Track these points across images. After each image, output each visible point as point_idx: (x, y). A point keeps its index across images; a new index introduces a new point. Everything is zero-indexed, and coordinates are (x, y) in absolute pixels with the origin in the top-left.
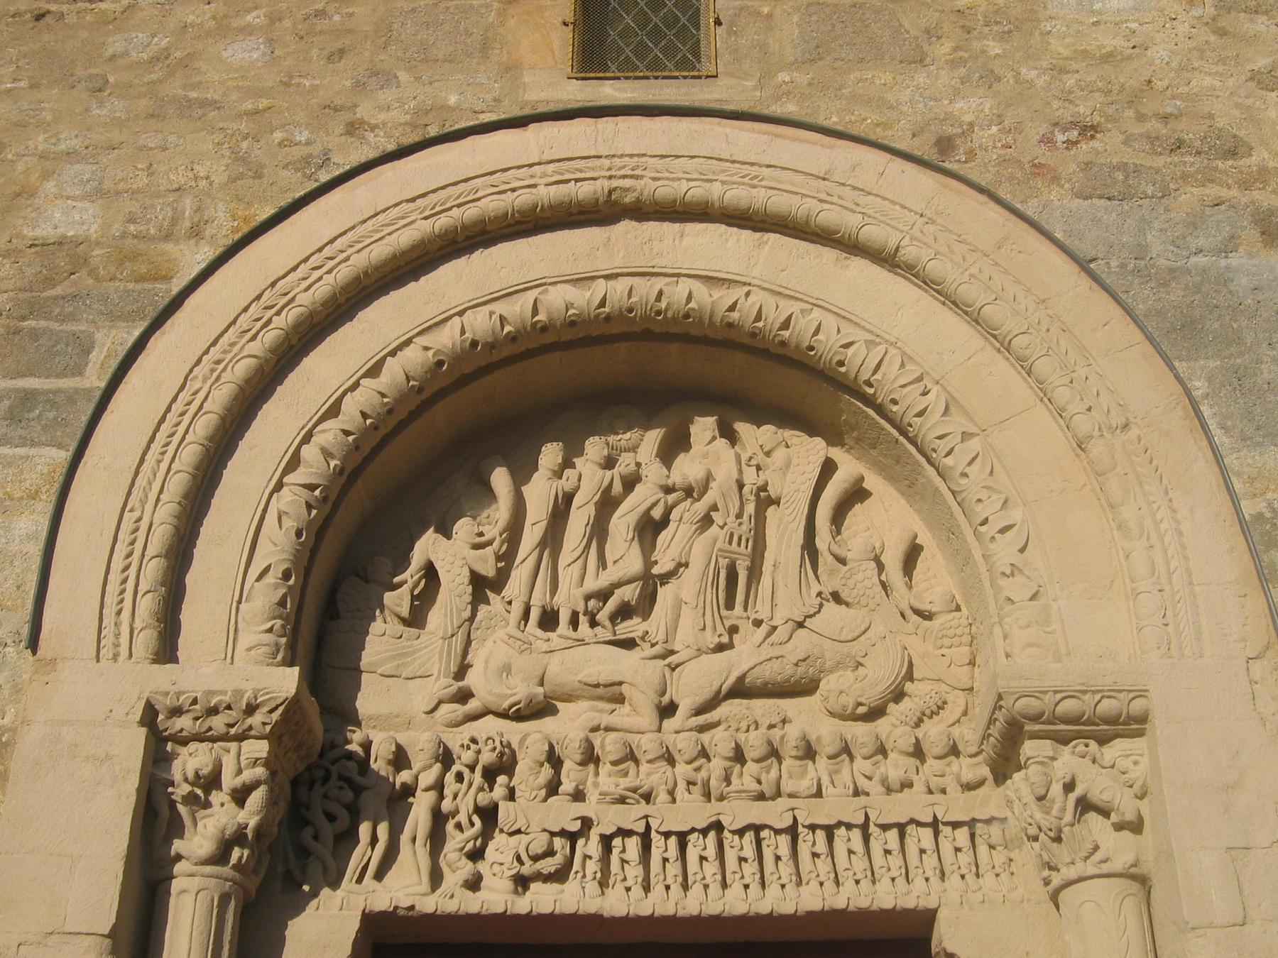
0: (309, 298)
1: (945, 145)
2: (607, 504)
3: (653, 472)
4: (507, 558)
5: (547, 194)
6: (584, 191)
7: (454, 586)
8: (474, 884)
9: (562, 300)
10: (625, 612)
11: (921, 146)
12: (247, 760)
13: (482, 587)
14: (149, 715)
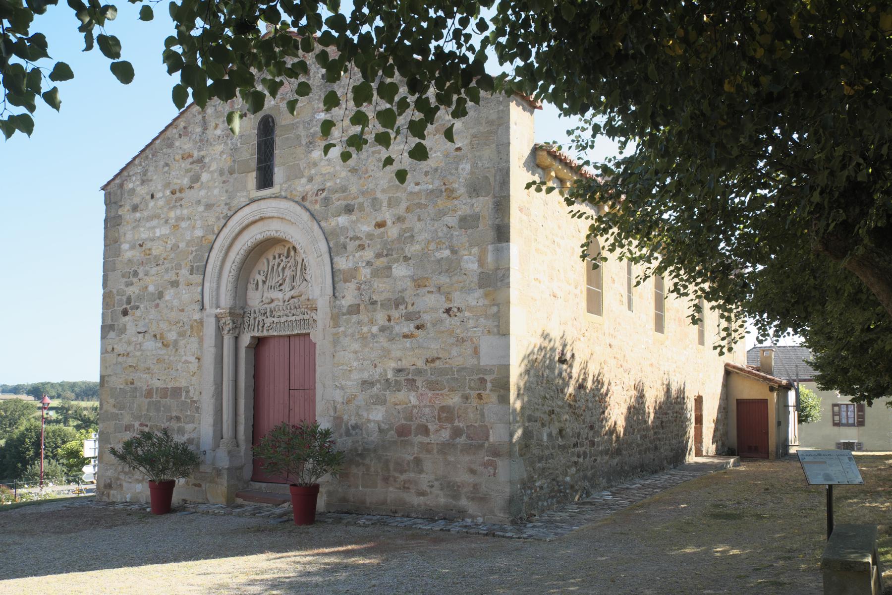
0: (227, 244)
1: (304, 198)
2: (279, 264)
3: (284, 259)
4: (266, 277)
5: (252, 219)
6: (257, 217)
7: (260, 283)
8: (262, 331)
9: (259, 237)
10: (281, 285)
11: (298, 199)
12: (228, 320)
13: (264, 282)
14: (216, 316)
